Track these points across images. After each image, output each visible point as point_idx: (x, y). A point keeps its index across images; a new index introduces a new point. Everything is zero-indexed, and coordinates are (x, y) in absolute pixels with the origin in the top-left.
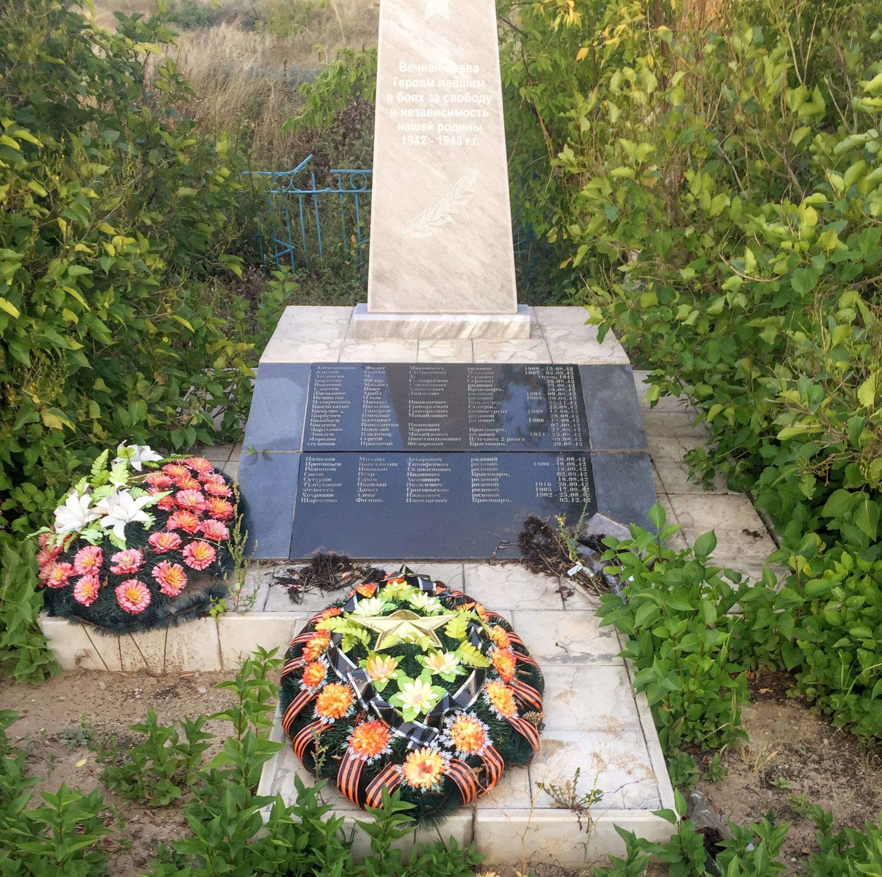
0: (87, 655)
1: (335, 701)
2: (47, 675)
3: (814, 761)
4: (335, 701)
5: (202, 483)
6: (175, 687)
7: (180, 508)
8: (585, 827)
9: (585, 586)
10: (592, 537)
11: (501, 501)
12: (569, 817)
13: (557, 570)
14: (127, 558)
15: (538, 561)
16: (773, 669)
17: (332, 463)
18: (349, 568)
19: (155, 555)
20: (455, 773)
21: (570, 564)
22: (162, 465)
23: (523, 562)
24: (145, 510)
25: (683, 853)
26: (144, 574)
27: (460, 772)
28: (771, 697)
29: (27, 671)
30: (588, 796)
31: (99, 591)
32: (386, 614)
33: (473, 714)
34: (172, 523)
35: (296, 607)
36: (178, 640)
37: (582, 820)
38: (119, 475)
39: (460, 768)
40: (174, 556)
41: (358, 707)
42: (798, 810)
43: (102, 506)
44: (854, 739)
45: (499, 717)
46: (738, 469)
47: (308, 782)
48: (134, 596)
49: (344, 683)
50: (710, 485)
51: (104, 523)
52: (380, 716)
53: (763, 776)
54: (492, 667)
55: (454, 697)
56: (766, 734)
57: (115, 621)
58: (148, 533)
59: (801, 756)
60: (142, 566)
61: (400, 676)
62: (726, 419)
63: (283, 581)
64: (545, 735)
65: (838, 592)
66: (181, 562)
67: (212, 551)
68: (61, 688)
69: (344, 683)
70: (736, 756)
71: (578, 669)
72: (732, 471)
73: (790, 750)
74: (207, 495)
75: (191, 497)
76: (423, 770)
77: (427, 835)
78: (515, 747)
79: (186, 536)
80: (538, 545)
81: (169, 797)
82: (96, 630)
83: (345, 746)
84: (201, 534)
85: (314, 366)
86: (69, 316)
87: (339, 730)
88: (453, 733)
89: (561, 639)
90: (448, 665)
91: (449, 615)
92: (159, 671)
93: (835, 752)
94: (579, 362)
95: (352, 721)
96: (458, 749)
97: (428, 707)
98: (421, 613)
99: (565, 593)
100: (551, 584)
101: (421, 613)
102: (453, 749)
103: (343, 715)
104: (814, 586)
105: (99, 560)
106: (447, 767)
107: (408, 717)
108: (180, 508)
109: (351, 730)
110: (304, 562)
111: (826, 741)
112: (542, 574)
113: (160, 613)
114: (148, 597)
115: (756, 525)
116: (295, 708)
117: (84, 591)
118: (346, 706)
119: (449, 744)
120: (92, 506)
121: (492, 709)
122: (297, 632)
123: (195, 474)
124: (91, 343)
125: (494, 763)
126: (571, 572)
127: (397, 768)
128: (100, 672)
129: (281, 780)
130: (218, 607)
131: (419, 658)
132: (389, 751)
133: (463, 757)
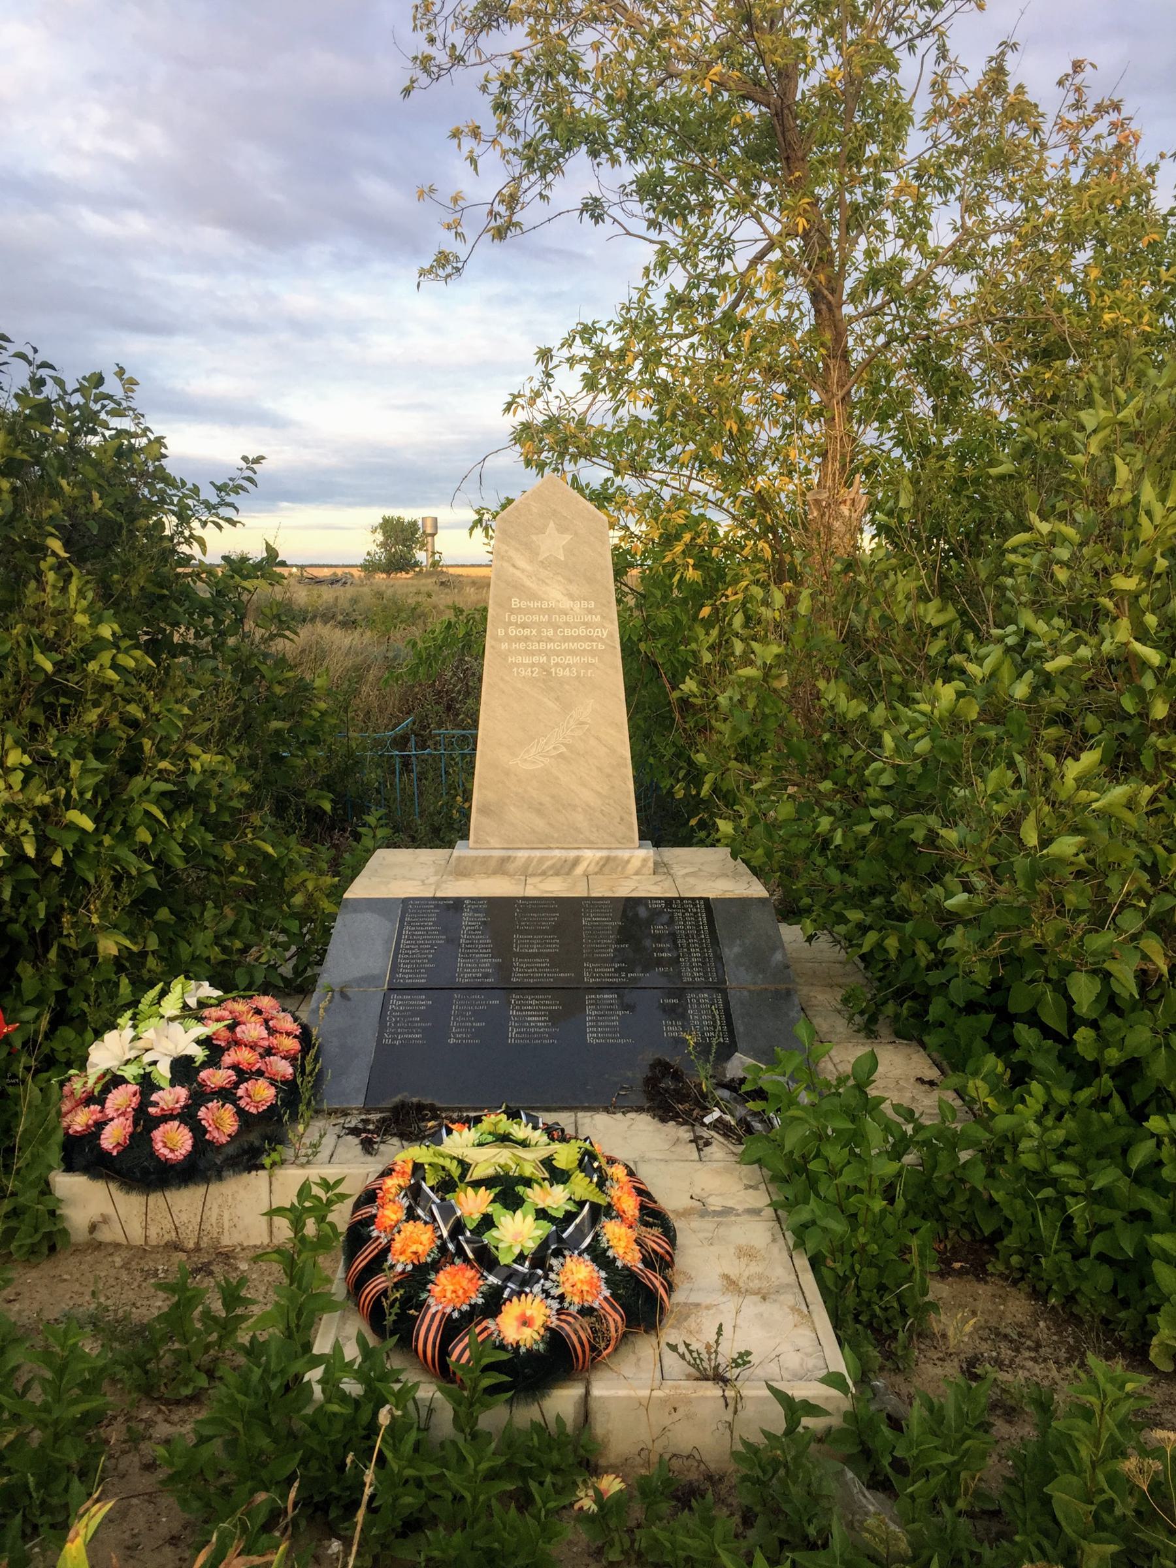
0: (105, 1220)
1: (414, 1241)
2: (52, 1249)
3: (1029, 1349)
4: (414, 1241)
5: (266, 1021)
6: (210, 1263)
7: (238, 1043)
8: (731, 1403)
9: (725, 1135)
10: (732, 1080)
11: (623, 1041)
12: (712, 1391)
13: (690, 1120)
14: (171, 1097)
15: (670, 1108)
16: (967, 1237)
17: (422, 1001)
18: (435, 1117)
19: (203, 1094)
20: (564, 1325)
21: (707, 1111)
22: (220, 1002)
23: (648, 1110)
24: (199, 1042)
25: (862, 1443)
26: (188, 1116)
27: (569, 1323)
28: (967, 1273)
29: (29, 1241)
30: (734, 1361)
31: (132, 1135)
32: (480, 1145)
33: (587, 1257)
34: (228, 1059)
35: (369, 1159)
36: (220, 1201)
37: (727, 1393)
38: (171, 1005)
39: (570, 1319)
40: (226, 1095)
41: (443, 1248)
42: (1012, 1403)
43: (151, 1039)
44: (1078, 1321)
45: (619, 1264)
46: (905, 1012)
47: (372, 1340)
48: (174, 1142)
49: (426, 1223)
50: (872, 1032)
51: (147, 1058)
52: (471, 1255)
53: (964, 1366)
54: (610, 1205)
55: (565, 1235)
56: (962, 1314)
57: (146, 1172)
58: (198, 1070)
59: (1011, 1342)
60: (186, 1106)
61: (497, 1210)
62: (886, 951)
63: (354, 1131)
64: (679, 1297)
65: (1032, 1127)
66: (234, 1101)
67: (273, 1091)
68: (67, 1266)
69: (426, 1223)
70: (928, 1342)
71: (719, 1224)
72: (897, 1016)
73: (998, 1334)
74: (272, 1031)
75: (253, 1030)
76: (522, 1323)
77: (526, 1414)
78: (641, 1302)
79: (243, 1074)
80: (666, 1090)
81: (192, 1385)
82: (120, 1188)
83: (424, 1296)
84: (260, 1073)
85: (405, 901)
86: (144, 836)
87: (420, 1276)
88: (561, 1279)
89: (697, 1191)
90: (556, 1198)
91: (556, 1146)
92: (191, 1245)
93: (1055, 1338)
94: (711, 896)
95: (435, 1266)
96: (568, 1300)
97: (531, 1246)
98: (524, 1144)
99: (701, 1143)
100: (684, 1133)
101: (524, 1144)
102: (562, 1298)
103: (423, 1260)
104: (1003, 1122)
105: (135, 1101)
106: (554, 1319)
107: (505, 1259)
108: (238, 1043)
109: (432, 1277)
110: (381, 1111)
111: (1042, 1324)
112: (672, 1123)
113: (202, 1164)
114: (190, 1142)
115: (933, 1074)
116: (361, 1262)
117: (112, 1137)
118: (427, 1248)
119: (555, 1292)
120: (136, 1038)
121: (610, 1253)
122: (371, 1179)
123: (258, 1012)
124: (162, 864)
125: (614, 1320)
126: (707, 1120)
127: (490, 1323)
128: (117, 1246)
129: (339, 1335)
130: (275, 1156)
131: (520, 1189)
132: (480, 1301)
133: (573, 1310)
